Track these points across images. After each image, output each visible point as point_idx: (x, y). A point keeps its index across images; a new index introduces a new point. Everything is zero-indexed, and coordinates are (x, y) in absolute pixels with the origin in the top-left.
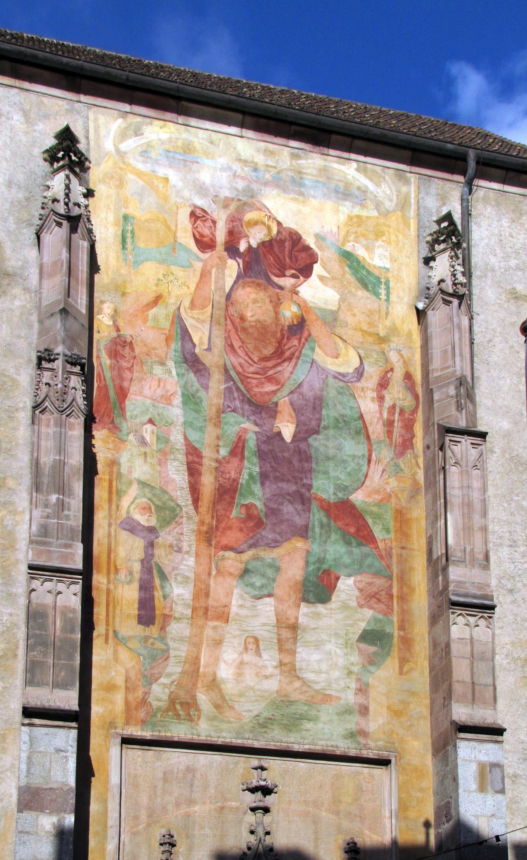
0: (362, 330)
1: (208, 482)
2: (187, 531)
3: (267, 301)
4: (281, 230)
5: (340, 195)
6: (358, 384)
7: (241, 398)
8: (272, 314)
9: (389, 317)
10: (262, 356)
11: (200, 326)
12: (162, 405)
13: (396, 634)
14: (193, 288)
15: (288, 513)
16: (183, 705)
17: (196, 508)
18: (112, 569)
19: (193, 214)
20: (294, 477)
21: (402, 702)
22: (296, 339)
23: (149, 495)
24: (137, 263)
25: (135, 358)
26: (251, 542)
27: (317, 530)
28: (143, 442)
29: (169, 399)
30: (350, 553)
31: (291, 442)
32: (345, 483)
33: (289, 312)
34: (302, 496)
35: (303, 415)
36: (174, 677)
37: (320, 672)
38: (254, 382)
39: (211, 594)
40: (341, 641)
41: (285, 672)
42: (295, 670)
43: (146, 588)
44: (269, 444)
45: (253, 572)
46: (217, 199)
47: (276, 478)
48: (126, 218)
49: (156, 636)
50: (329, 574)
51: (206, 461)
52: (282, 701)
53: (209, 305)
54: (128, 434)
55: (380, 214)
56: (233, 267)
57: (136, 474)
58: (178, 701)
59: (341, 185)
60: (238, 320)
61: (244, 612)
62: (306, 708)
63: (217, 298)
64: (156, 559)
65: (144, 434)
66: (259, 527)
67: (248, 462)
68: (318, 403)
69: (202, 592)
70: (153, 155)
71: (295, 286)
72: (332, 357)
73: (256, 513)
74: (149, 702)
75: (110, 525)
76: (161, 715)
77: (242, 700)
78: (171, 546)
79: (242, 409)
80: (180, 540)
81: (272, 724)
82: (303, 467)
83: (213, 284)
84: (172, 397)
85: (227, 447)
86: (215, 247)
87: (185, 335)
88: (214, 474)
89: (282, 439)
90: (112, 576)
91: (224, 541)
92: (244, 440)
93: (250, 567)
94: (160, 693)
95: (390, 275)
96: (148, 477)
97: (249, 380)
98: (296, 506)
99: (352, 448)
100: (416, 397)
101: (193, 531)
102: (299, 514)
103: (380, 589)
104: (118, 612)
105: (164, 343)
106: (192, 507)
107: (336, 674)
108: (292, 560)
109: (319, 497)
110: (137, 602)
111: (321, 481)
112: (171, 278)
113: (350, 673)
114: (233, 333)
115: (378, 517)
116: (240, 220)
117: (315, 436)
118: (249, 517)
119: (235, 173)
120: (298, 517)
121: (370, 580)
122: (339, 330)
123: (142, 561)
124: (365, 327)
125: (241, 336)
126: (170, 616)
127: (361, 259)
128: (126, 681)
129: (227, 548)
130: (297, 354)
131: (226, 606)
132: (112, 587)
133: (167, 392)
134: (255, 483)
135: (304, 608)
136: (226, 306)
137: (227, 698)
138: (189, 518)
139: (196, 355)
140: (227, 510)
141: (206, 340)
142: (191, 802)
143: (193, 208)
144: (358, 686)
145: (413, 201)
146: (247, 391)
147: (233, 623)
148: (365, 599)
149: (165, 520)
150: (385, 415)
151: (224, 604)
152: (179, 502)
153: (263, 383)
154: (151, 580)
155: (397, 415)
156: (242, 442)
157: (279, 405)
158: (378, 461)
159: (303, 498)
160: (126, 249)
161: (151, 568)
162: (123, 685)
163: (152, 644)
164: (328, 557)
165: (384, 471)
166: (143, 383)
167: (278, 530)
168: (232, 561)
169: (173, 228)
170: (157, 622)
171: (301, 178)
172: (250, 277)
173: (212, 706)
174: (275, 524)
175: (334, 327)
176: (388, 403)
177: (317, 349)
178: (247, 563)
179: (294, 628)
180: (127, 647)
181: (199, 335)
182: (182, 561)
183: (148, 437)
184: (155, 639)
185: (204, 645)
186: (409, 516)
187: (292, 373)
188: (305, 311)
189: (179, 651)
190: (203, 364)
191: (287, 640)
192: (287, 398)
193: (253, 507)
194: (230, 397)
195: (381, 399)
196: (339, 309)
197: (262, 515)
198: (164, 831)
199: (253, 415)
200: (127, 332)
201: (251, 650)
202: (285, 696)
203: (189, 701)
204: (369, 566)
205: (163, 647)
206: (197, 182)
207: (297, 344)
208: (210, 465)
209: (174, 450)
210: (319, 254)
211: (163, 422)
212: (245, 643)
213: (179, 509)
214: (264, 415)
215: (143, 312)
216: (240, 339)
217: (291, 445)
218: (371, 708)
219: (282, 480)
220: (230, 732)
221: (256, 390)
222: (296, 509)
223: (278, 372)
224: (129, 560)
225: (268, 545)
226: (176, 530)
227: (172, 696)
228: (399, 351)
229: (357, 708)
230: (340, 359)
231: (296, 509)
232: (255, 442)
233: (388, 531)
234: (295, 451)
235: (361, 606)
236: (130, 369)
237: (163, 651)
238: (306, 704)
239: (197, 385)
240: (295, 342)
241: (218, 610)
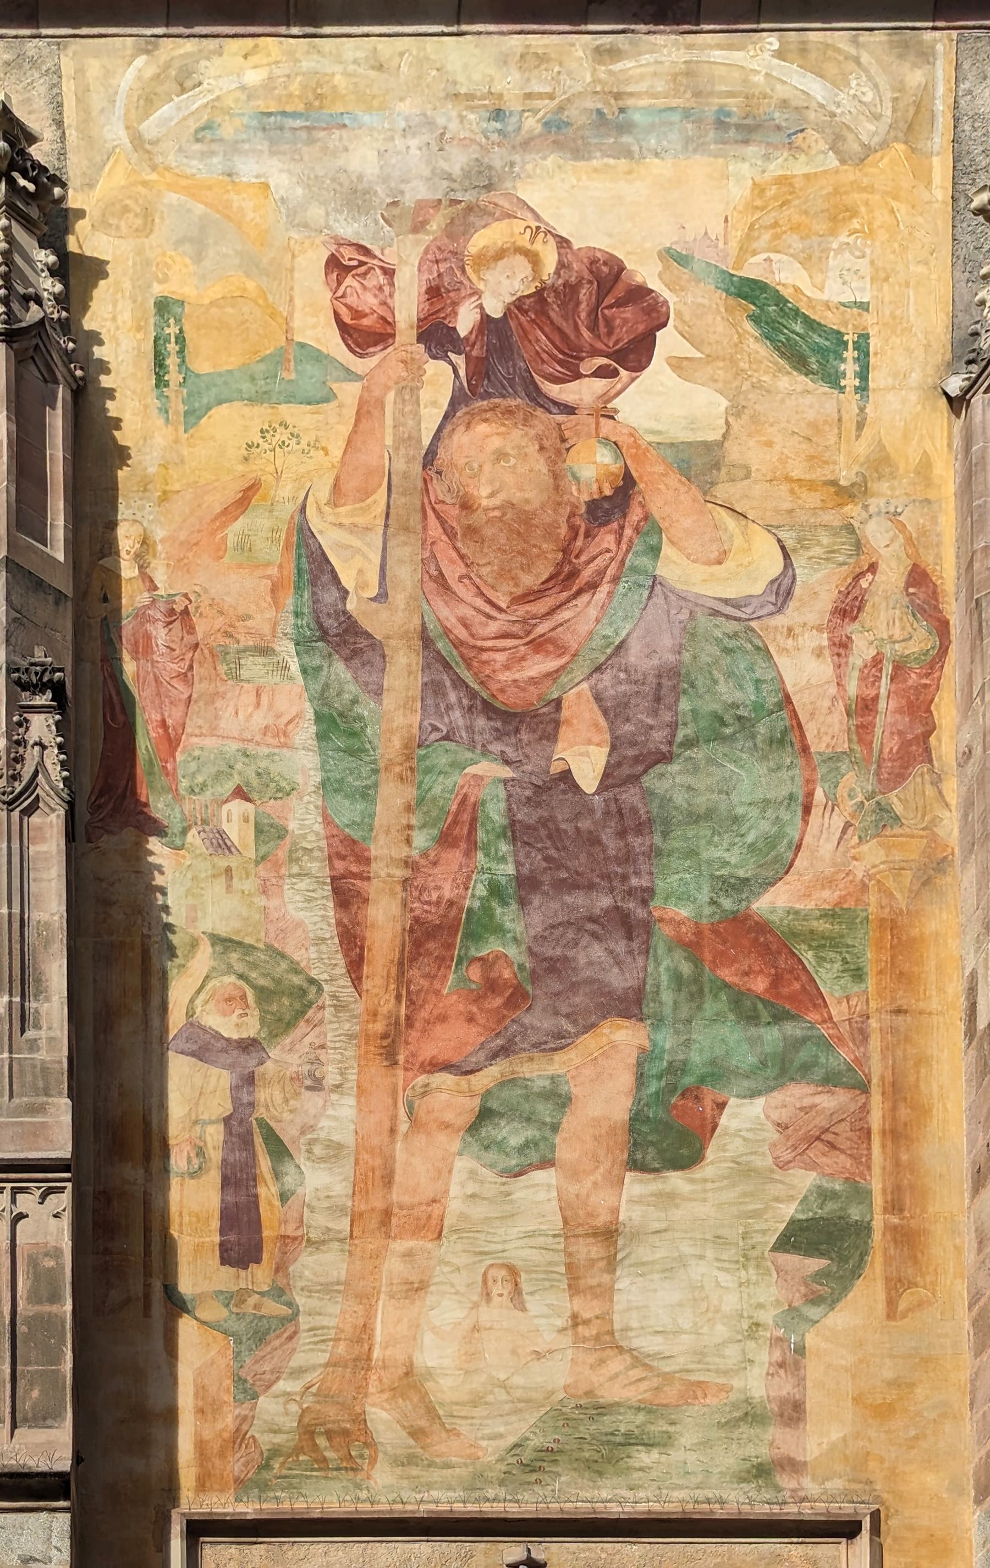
1: (384, 917)
3: (533, 448)
5: (732, 133)
7: (465, 702)
10: (519, 591)
14: (337, 452)
17: (357, 981)
19: (335, 265)
20: (608, 877)
21: (895, 1383)
22: (610, 532)
24: (193, 416)
27: (667, 996)
29: (285, 734)
31: (598, 792)
35: (628, 720)
38: (501, 657)
39: (397, 1178)
44: (538, 805)
45: (502, 1115)
46: (396, 211)
47: (562, 886)
51: (378, 869)
53: (380, 485)
56: (440, 379)
59: (733, 104)
60: (455, 511)
61: (478, 1211)
63: (400, 465)
66: (516, 1007)
67: (487, 855)
70: (227, 130)
71: (607, 398)
73: (507, 974)
77: (479, 1412)
79: (470, 729)
82: (629, 849)
83: (389, 431)
84: (290, 727)
85: (434, 826)
86: (393, 336)
88: (400, 894)
89: (576, 788)
91: (428, 1051)
93: (494, 1104)
95: (869, 319)
96: (237, 924)
97: (485, 656)
98: (612, 945)
100: (942, 628)
102: (618, 963)
105: (269, 599)
108: (602, 1074)
109: (671, 914)
111: (677, 877)
112: (282, 435)
114: (445, 552)
115: (823, 943)
117: (659, 768)
118: (491, 986)
119: (443, 134)
120: (616, 970)
125: (464, 551)
129: (435, 1066)
130: (610, 572)
136: (425, 481)
137: (441, 1413)
138: (340, 1007)
140: (435, 976)
141: (374, 578)
143: (333, 248)
145: (940, 106)
146: (482, 683)
147: (456, 1236)
151: (431, 1196)
153: (523, 658)
154: (251, 1163)
155: (885, 682)
156: (469, 809)
157: (565, 704)
159: (632, 927)
160: (167, 385)
166: (218, 704)
167: (564, 1009)
168: (451, 1097)
169: (283, 309)
172: (487, 396)
174: (557, 994)
176: (862, 651)
178: (488, 1094)
181: (355, 567)
188: (635, 457)
190: (369, 636)
193: (501, 962)
194: (437, 706)
195: (842, 646)
196: (725, 436)
199: (498, 739)
201: (501, 1295)
206: (343, 178)
207: (613, 547)
208: (389, 875)
209: (300, 854)
211: (271, 791)
212: (485, 1282)
215: (213, 533)
216: (462, 557)
219: (575, 886)
220: (450, 1488)
221: (506, 677)
222: (611, 952)
223: (561, 625)
231: (611, 952)
234: (607, 813)
237: (284, 1320)
239: (352, 689)
241: (415, 1212)
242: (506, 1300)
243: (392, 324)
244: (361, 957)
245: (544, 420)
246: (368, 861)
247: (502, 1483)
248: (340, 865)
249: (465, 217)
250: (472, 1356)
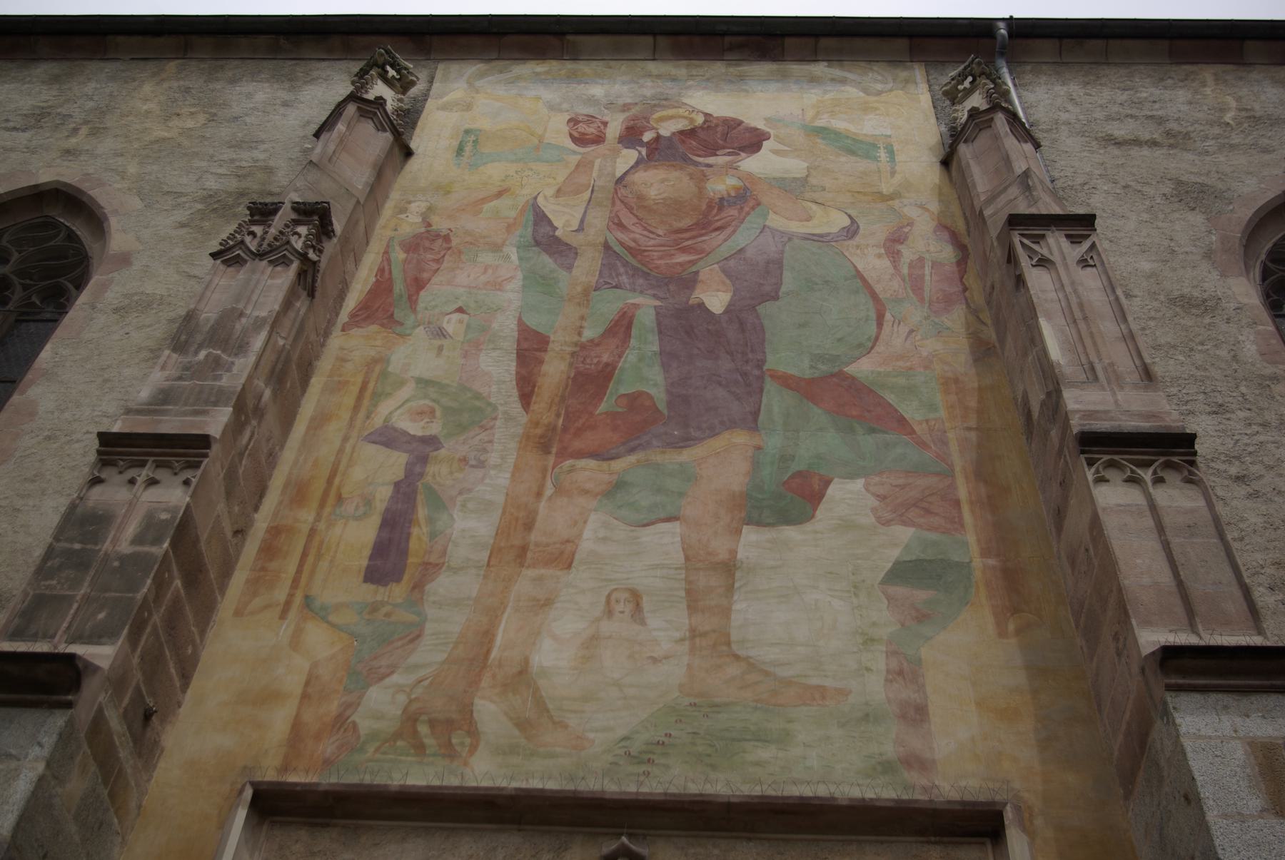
1: (554, 370)
3: (686, 179)
6: (850, 242)
13: (977, 563)
18: (331, 500)
19: (574, 121)
25: (449, 248)
28: (441, 333)
33: (721, 185)
36: (422, 673)
39: (539, 524)
42: (729, 644)
49: (399, 601)
54: (414, 327)
57: (416, 373)
58: (424, 718)
64: (428, 479)
65: (445, 325)
68: (774, 266)
74: (354, 723)
75: (346, 439)
76: (377, 750)
78: (464, 460)
87: (540, 218)
90: (328, 510)
91: (577, 444)
92: (632, 317)
94: (382, 704)
104: (324, 565)
108: (724, 462)
110: (370, 545)
113: (869, 641)
121: (901, 481)
123: (397, 485)
128: (307, 683)
129: (580, 455)
131: (568, 541)
132: (322, 526)
135: (750, 535)
137: (550, 706)
152: (493, 400)
161: (415, 492)
162: (298, 691)
163: (388, 615)
165: (911, 331)
168: (588, 472)
170: (406, 577)
179: (729, 568)
180: (328, 622)
183: (450, 328)
185: (509, 610)
187: (725, 240)
197: (662, 406)
201: (622, 612)
205: (412, 618)
210: (772, 132)
213: (489, 409)
226: (479, 437)
228: (922, 207)
233: (932, 407)
235: (887, 523)
238: (756, 708)
244: (532, 392)
245: (691, 169)
248: (525, 345)
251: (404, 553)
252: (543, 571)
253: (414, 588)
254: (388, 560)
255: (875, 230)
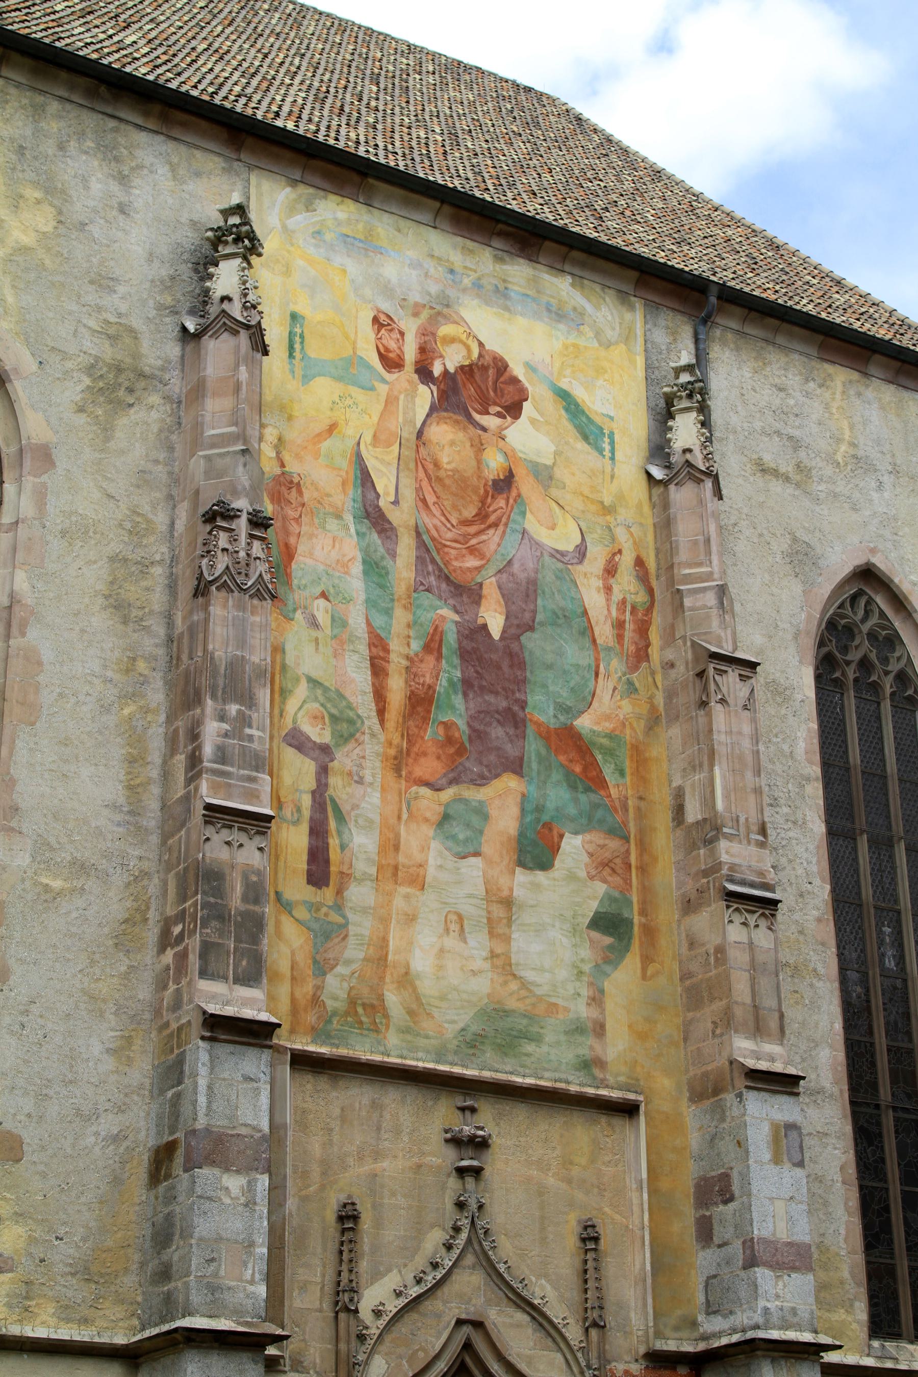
0: (583, 495)
1: (396, 687)
2: (368, 755)
3: (468, 444)
4: (484, 353)
6: (579, 568)
8: (474, 463)
9: (615, 480)
11: (384, 469)
12: (338, 574)
13: (636, 920)
15: (498, 738)
16: (367, 1011)
17: (382, 721)
20: (504, 689)
23: (321, 698)
26: (451, 775)
27: (534, 766)
28: (314, 624)
30: (576, 801)
32: (568, 703)
33: (494, 463)
34: (514, 715)
36: (354, 966)
37: (542, 970)
38: (453, 552)
39: (402, 847)
40: (567, 926)
41: (497, 967)
42: (510, 965)
43: (318, 831)
44: (472, 640)
45: (455, 819)
48: (294, 317)
49: (331, 904)
50: (550, 830)
51: (393, 657)
52: (495, 1009)
54: (295, 610)
55: (600, 345)
56: (425, 395)
62: (525, 1022)
63: (405, 435)
64: (330, 792)
65: (316, 613)
69: (390, 845)
72: (548, 528)
73: (457, 735)
78: (350, 774)
79: (439, 588)
80: (360, 766)
81: (483, 1043)
87: (365, 479)
88: (404, 675)
89: (489, 635)
91: (418, 772)
92: (442, 632)
93: (451, 812)
94: (336, 987)
97: (446, 550)
99: (575, 654)
101: (378, 754)
102: (511, 741)
103: (616, 854)
106: (375, 720)
107: (563, 974)
113: (581, 973)
115: (609, 753)
116: (434, 335)
117: (528, 634)
118: (449, 740)
121: (601, 842)
122: (554, 492)
124: (586, 492)
126: (349, 875)
127: (579, 401)
128: (292, 968)
130: (504, 520)
133: (344, 556)
134: (456, 693)
135: (521, 876)
138: (373, 735)
139: (380, 510)
142: (378, 1155)
144: (591, 993)
147: (430, 890)
148: (597, 868)
149: (342, 736)
150: (614, 613)
152: (360, 712)
158: (608, 676)
159: (515, 719)
161: (325, 803)
163: (326, 915)
164: (548, 804)
165: (615, 689)
167: (485, 763)
168: (430, 802)
171: (506, 288)
172: (446, 410)
173: (404, 1012)
175: (549, 487)
177: (528, 515)
178: (447, 805)
179: (508, 903)
181: (384, 483)
182: (364, 796)
184: (330, 907)
185: (393, 921)
186: (647, 755)
187: (499, 545)
189: (361, 927)
190: (390, 523)
191: (501, 919)
192: (493, 579)
198: (343, 1198)
200: (293, 467)
202: (498, 1002)
203: (375, 1002)
204: (601, 822)
205: (340, 920)
210: (530, 389)
212: (446, 921)
214: (465, 599)
216: (435, 492)
217: (501, 644)
218: (607, 1027)
220: (428, 1052)
221: (456, 563)
224: (297, 790)
225: (473, 782)
226: (356, 751)
227: (353, 993)
229: (590, 1025)
230: (557, 530)
231: (507, 734)
232: (455, 636)
233: (622, 773)
235: (592, 878)
236: (298, 520)
239: (381, 550)
240: (502, 503)
241: (411, 870)
242: (456, 934)
243: (403, 360)
246: (387, 651)
247: (456, 1053)
249: (437, 317)
250: (440, 967)
251: (327, 862)
252: (408, 890)
253: (338, 893)
254: (319, 869)
255: (597, 555)
